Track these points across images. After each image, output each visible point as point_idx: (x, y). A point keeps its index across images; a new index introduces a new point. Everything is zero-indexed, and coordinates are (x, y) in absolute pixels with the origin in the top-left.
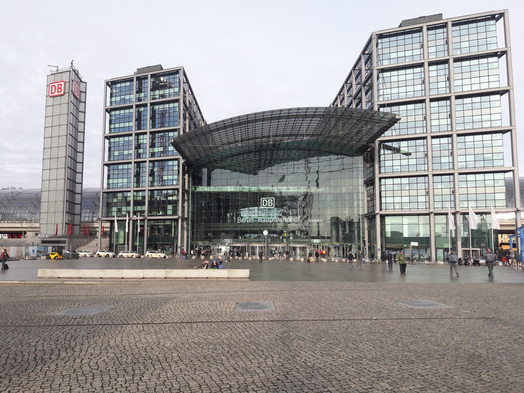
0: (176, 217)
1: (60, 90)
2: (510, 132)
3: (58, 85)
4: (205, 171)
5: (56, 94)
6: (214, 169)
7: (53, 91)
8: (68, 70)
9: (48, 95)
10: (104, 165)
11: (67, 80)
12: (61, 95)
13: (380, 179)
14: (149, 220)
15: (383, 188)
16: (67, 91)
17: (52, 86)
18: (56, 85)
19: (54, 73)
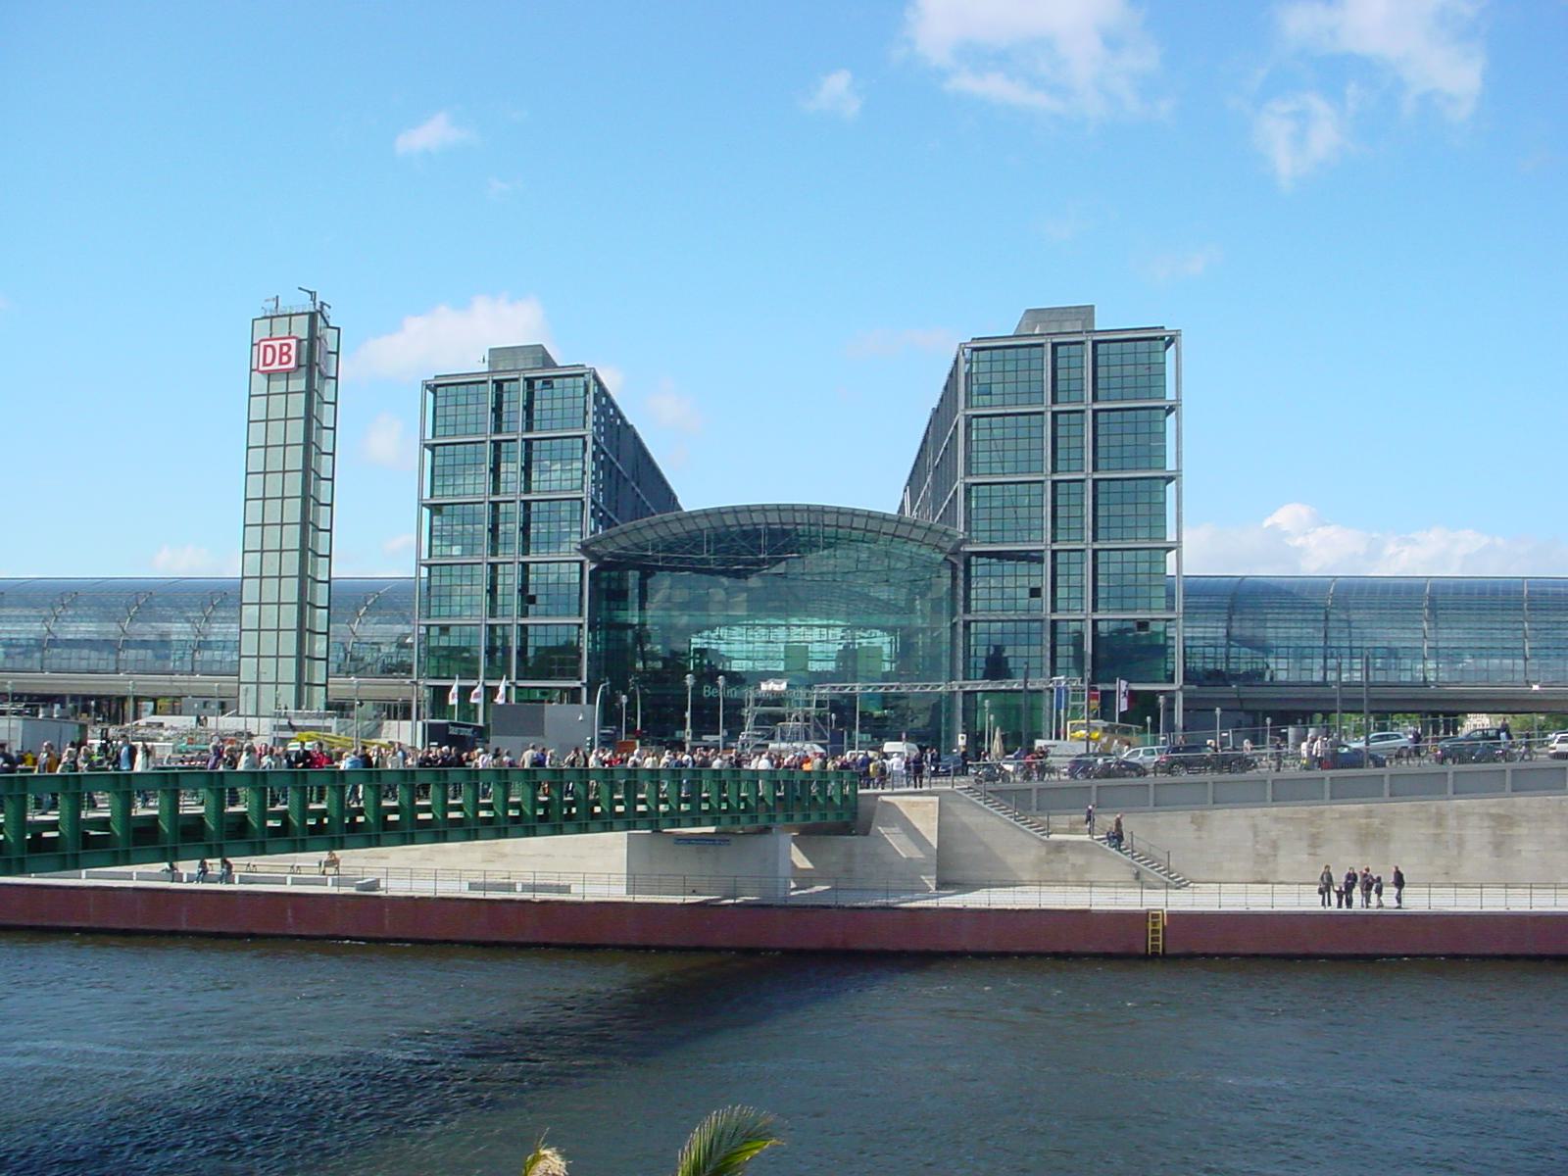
0: (578, 684)
1: (285, 359)
2: (1174, 552)
3: (281, 346)
4: (633, 576)
5: (276, 366)
6: (652, 574)
7: (268, 361)
8: (306, 311)
9: (254, 367)
10: (422, 565)
11: (304, 335)
12: (288, 372)
13: (967, 625)
14: (518, 688)
15: (972, 642)
16: (304, 361)
17: (266, 347)
19: (268, 314)
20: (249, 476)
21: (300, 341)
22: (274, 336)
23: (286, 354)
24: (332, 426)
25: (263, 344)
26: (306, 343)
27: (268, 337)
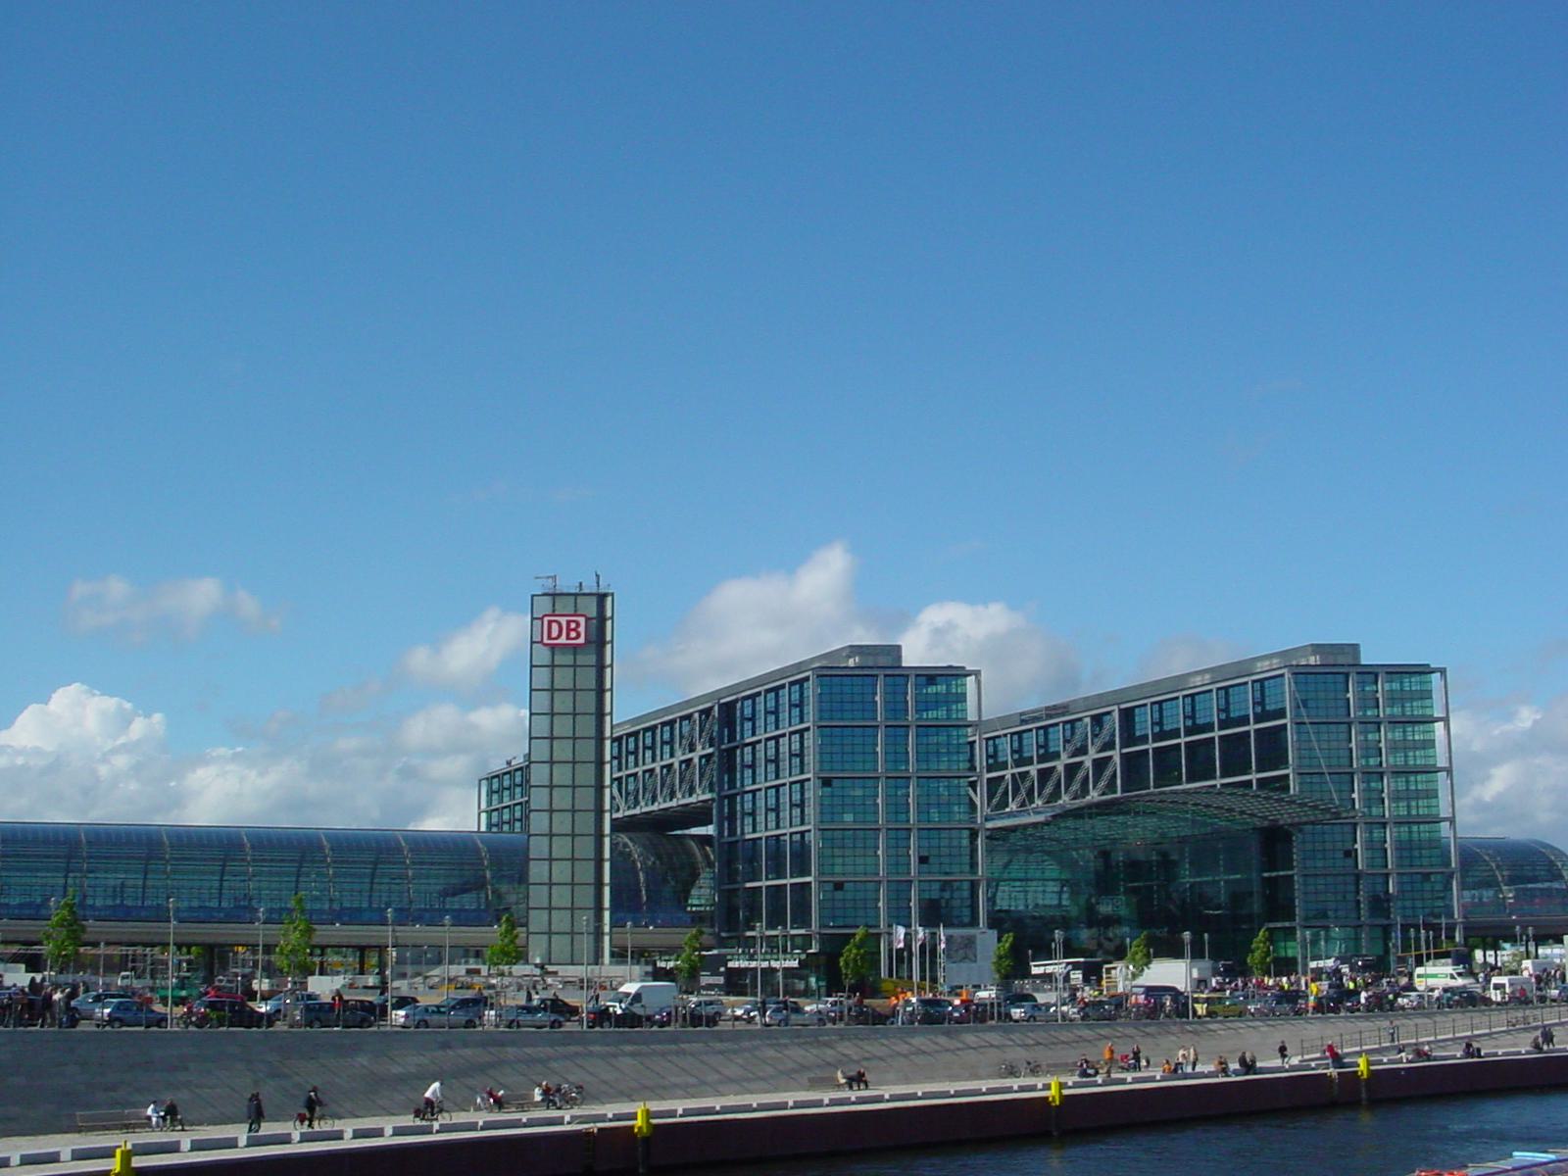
1: (573, 634)
3: (568, 622)
5: (563, 640)
7: (555, 633)
9: (537, 638)
11: (593, 612)
16: (594, 637)
17: (550, 622)
18: (563, 620)
20: (533, 741)
21: (592, 619)
22: (557, 613)
23: (574, 630)
24: (533, 693)
25: (546, 619)
26: (594, 621)
27: (550, 612)
